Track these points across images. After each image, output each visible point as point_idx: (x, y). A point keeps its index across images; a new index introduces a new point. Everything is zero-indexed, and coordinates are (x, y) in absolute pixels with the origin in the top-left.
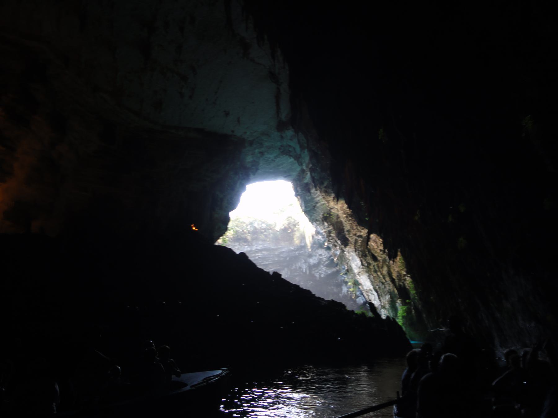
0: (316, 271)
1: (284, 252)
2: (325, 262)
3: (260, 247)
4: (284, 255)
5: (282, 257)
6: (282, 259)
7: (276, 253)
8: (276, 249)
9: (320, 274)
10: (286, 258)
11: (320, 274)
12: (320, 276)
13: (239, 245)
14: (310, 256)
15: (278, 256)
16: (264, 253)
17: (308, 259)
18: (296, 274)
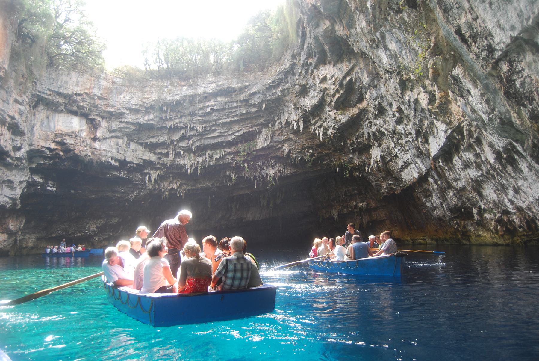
0: (318, 124)
1: (254, 94)
2: (334, 96)
3: (210, 88)
4: (255, 100)
5: (254, 106)
6: (254, 110)
7: (242, 97)
8: (241, 90)
9: (326, 129)
10: (261, 104)
11: (326, 129)
12: (325, 134)
13: (172, 84)
14: (304, 91)
15: (246, 102)
16: (220, 99)
17: (301, 100)
18: (282, 138)
